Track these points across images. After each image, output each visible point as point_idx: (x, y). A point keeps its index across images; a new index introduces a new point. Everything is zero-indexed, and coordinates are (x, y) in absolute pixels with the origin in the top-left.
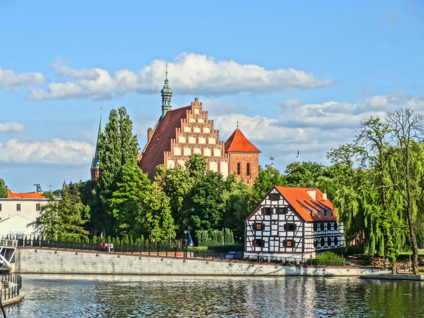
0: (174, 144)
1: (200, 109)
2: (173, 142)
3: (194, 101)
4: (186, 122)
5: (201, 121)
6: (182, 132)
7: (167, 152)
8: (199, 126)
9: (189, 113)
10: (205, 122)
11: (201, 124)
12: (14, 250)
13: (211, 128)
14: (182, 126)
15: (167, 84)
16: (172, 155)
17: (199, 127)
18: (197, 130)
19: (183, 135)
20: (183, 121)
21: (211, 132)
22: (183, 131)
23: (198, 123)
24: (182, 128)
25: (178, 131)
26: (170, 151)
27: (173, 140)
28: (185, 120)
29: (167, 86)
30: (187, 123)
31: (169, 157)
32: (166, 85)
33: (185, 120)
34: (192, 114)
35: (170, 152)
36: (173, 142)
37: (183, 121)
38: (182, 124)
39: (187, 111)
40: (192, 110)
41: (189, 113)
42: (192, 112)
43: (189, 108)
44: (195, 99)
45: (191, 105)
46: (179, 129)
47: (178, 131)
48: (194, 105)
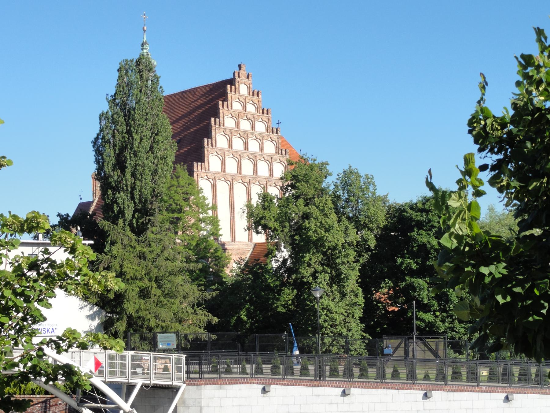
0: (209, 150)
1: (248, 86)
2: (208, 145)
3: (237, 70)
4: (228, 107)
5: (251, 109)
6: (222, 127)
7: (199, 164)
8: (248, 117)
9: (231, 91)
10: (257, 110)
11: (251, 114)
12: (176, 390)
13: (268, 123)
14: (221, 115)
15: (146, 49)
16: (207, 171)
17: (248, 119)
18: (245, 125)
19: (223, 133)
20: (223, 106)
21: (267, 131)
22: (224, 126)
23: (247, 113)
24: (221, 119)
25: (215, 124)
26: (204, 162)
27: (208, 141)
28: (225, 103)
29: (147, 52)
30: (230, 110)
31: (202, 175)
32: (145, 51)
33: (225, 103)
34: (237, 93)
35: (203, 164)
36: (208, 145)
37: (223, 106)
38: (221, 111)
39: (229, 86)
40: (237, 84)
41: (231, 91)
42: (237, 90)
43: (231, 82)
44: (240, 66)
45: (231, 76)
46: (217, 120)
47: (215, 124)
48: (239, 77)
